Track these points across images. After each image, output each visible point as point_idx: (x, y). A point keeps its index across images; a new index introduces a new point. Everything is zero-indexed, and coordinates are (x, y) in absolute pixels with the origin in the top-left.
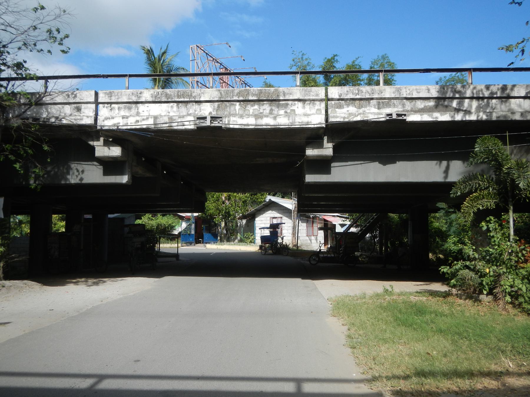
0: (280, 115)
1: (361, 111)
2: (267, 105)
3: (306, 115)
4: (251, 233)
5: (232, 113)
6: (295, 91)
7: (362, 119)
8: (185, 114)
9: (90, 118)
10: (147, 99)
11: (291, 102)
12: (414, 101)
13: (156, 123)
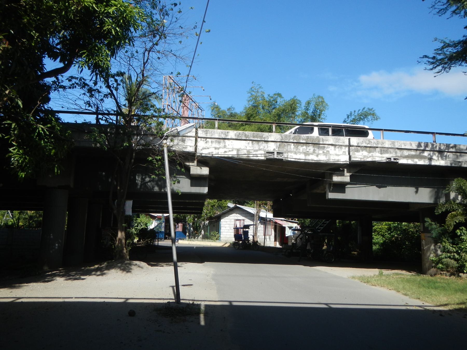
0: (320, 154)
1: (370, 154)
2: (312, 147)
3: (336, 155)
4: (216, 232)
5: (288, 150)
6: (330, 139)
7: (372, 160)
8: (257, 149)
9: (192, 148)
10: (232, 137)
11: (327, 146)
12: (402, 151)
13: (238, 154)
